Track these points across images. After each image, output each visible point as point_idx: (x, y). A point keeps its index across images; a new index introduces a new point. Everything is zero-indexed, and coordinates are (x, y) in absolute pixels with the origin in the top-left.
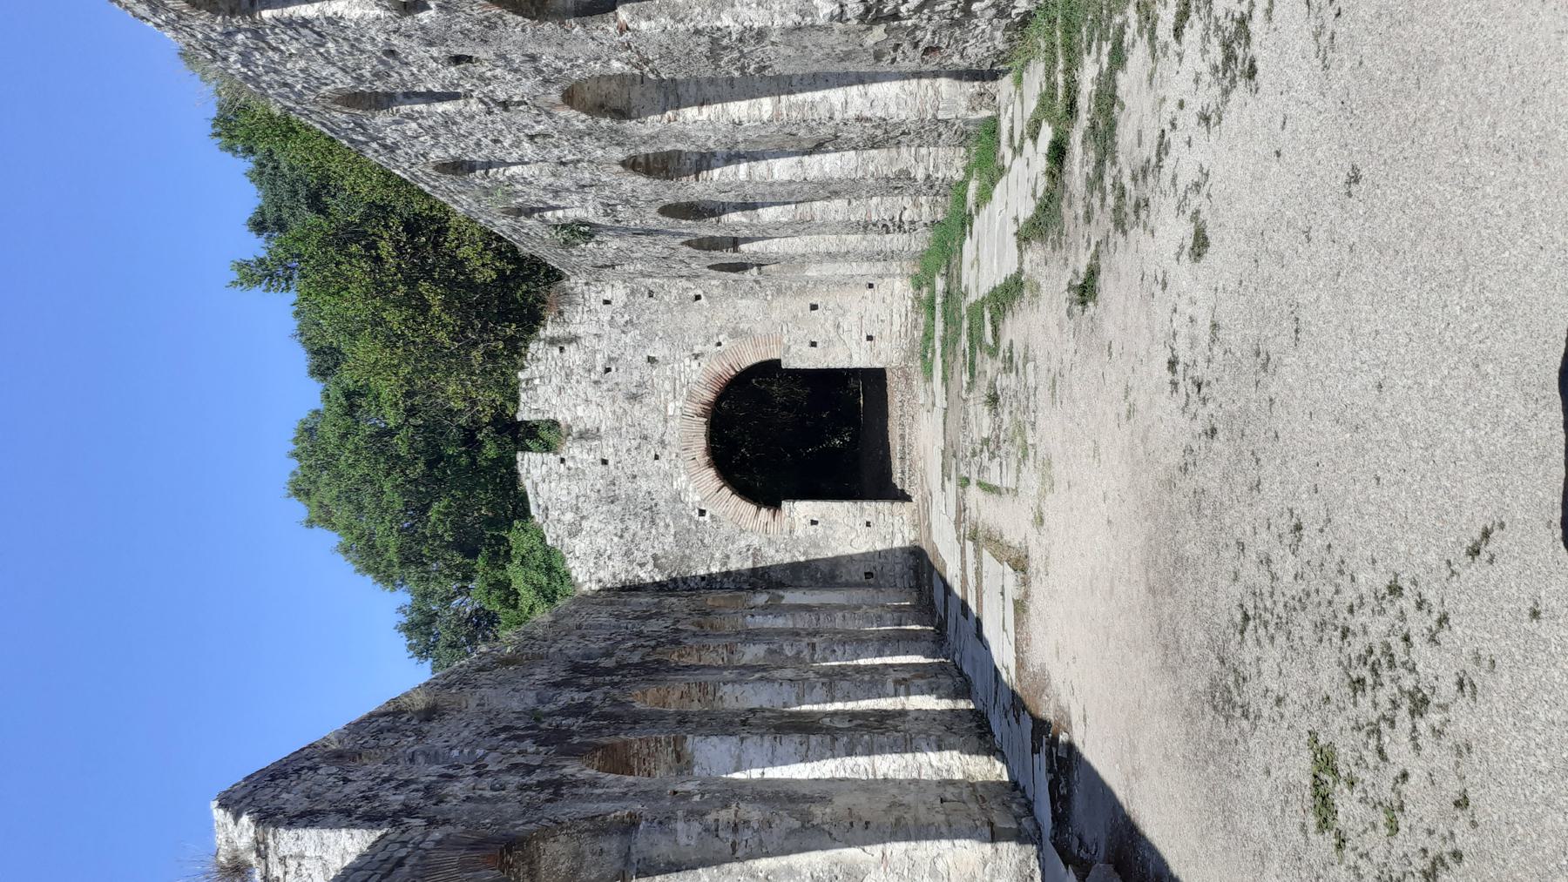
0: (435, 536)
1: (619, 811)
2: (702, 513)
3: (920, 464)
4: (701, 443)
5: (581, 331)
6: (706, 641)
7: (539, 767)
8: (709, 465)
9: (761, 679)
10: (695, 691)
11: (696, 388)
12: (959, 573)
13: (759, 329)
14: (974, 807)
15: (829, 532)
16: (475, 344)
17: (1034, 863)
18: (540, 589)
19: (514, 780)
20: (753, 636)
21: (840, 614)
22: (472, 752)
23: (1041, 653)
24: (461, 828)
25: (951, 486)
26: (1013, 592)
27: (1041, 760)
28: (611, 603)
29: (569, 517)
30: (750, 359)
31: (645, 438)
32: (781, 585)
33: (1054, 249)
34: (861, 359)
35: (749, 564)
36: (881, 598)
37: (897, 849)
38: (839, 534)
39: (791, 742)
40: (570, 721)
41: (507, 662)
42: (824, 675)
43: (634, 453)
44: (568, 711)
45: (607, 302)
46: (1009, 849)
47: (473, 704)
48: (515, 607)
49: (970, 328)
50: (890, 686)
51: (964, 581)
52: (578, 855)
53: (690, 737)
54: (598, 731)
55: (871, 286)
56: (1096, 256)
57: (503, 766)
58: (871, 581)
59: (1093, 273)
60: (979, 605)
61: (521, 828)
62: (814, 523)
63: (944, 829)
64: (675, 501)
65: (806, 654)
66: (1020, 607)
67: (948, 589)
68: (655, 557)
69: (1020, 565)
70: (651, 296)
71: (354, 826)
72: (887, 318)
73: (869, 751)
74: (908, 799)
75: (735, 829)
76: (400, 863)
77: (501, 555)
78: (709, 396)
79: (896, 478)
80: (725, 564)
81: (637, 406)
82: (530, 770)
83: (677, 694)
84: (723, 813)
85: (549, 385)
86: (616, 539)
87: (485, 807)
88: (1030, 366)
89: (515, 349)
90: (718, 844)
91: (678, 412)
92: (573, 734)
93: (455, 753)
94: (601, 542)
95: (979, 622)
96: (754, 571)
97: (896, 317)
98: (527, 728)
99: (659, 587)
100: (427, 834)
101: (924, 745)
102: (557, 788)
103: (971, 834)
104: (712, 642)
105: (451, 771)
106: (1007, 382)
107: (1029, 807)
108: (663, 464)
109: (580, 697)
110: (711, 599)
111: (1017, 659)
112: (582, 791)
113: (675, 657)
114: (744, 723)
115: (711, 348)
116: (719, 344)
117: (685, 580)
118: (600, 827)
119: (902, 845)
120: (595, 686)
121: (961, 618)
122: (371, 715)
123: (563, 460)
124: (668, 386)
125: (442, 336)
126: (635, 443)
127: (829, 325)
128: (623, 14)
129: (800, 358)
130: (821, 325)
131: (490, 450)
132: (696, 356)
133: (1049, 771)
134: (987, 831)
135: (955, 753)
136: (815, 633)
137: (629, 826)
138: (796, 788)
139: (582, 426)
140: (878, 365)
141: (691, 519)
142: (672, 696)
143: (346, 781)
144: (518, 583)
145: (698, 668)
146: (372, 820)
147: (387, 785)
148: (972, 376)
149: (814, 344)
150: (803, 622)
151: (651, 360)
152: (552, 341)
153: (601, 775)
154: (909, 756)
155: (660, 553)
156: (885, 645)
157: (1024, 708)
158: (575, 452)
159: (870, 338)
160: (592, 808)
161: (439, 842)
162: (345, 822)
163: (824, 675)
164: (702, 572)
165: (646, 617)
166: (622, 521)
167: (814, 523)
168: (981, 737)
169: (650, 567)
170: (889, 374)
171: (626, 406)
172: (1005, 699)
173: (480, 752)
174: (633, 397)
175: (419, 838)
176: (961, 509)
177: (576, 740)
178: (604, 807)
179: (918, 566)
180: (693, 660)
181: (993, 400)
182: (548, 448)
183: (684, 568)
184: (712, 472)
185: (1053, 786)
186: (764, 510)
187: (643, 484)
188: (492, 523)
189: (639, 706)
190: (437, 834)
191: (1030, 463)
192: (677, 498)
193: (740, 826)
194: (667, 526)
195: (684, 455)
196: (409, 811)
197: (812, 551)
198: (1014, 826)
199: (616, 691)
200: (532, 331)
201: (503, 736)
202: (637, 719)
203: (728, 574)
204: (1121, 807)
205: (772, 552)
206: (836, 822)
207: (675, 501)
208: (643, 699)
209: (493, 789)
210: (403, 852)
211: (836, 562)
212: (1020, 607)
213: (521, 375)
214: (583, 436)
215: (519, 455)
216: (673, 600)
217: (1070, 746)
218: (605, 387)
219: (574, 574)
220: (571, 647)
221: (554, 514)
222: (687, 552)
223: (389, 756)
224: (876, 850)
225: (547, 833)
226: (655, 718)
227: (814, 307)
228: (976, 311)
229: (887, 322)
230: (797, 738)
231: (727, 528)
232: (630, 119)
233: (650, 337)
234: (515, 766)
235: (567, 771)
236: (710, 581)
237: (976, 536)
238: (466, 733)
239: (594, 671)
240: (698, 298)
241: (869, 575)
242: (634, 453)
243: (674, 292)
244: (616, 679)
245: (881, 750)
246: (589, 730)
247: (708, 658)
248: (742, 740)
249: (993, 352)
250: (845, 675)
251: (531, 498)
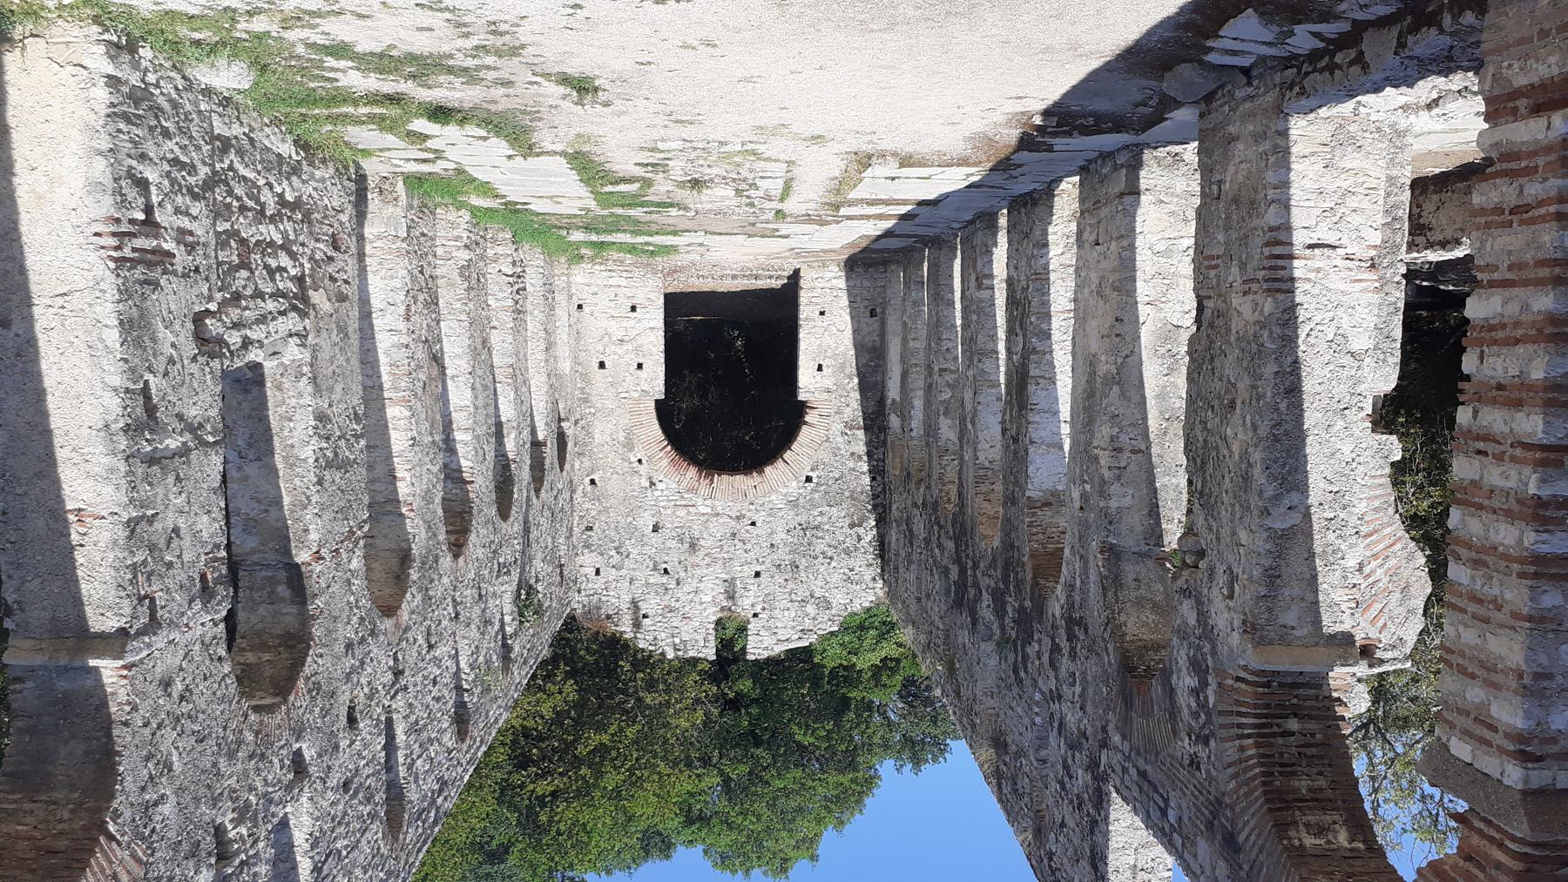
0: (828, 738)
1: (1097, 562)
3: (762, 259)
4: (739, 480)
5: (627, 598)
6: (935, 477)
7: (1053, 640)
8: (761, 472)
9: (973, 423)
10: (983, 488)
11: (684, 484)
12: (872, 222)
13: (624, 421)
14: (1104, 212)
16: (640, 700)
17: (1161, 152)
18: (881, 637)
19: (1065, 664)
20: (931, 430)
21: (911, 343)
22: (1037, 703)
23: (953, 141)
24: (1111, 716)
25: (785, 228)
26: (891, 168)
27: (1059, 143)
28: (896, 568)
29: (811, 609)
30: (655, 431)
31: (734, 535)
32: (881, 401)
33: (540, 119)
34: (655, 318)
35: (861, 434)
36: (896, 302)
37: (1143, 290)
39: (1035, 394)
40: (1009, 609)
41: (951, 670)
42: (971, 360)
43: (748, 546)
44: (1000, 611)
45: (598, 572)
46: (1146, 178)
47: (991, 703)
48: (898, 661)
49: (623, 206)
50: (985, 294)
51: (880, 217)
52: (1140, 603)
53: (1028, 494)
54: (1019, 583)
55: (580, 307)
56: (547, 76)
57: (1052, 674)
58: (878, 310)
59: (565, 80)
60: (904, 202)
61: (1111, 658)
62: (820, 368)
63: (1125, 243)
64: (796, 506)
65: (949, 378)
66: (906, 161)
67: (888, 234)
68: (852, 526)
69: (864, 161)
70: (591, 529)
71: (1107, 817)
72: (611, 293)
73: (1047, 316)
74: (1094, 277)
75: (1118, 450)
76: (1143, 774)
77: (846, 675)
78: (692, 472)
79: (776, 284)
81: (702, 542)
82: (1056, 649)
83: (986, 504)
84: (1102, 462)
85: (680, 629)
87: (1090, 691)
88: (660, 145)
89: (645, 661)
90: (1133, 468)
91: (708, 502)
92: (1022, 607)
93: (1038, 720)
94: (835, 578)
95: (921, 203)
96: (866, 428)
97: (611, 282)
98: (1016, 651)
99: (881, 522)
100: (1116, 748)
101: (1043, 261)
102: (1074, 623)
103: (1130, 215)
105: (1056, 725)
106: (678, 169)
107: (1106, 156)
108: (759, 518)
109: (986, 599)
110: (894, 470)
111: (959, 165)
112: (1077, 598)
113: (950, 507)
114: (1016, 440)
115: (643, 469)
117: (875, 497)
118: (1113, 581)
119: (1139, 284)
120: (976, 585)
121: (917, 221)
122: (1000, 800)
123: (755, 615)
124: (682, 512)
125: (631, 732)
126: (739, 545)
127: (620, 350)
128: (302, 557)
129: (654, 381)
130: (620, 359)
131: (745, 685)
132: (652, 484)
133: (1070, 135)
134: (1128, 199)
135: (1050, 229)
136: (929, 368)
137: (1112, 553)
138: (1080, 390)
139: (722, 597)
140: (662, 301)
142: (987, 510)
143: (1063, 825)
144: (875, 658)
145: (961, 485)
146: (1101, 801)
147: (1068, 786)
148: (671, 205)
149: (640, 366)
150: (918, 381)
151: (656, 529)
152: (637, 625)
153: (1062, 580)
154: (1052, 276)
155: (848, 521)
156: (942, 299)
157: (1008, 159)
158: (746, 604)
159: (633, 309)
160: (1094, 589)
161: (1124, 737)
162: (1102, 826)
163: (971, 360)
164: (867, 480)
165: (910, 535)
166: (815, 558)
167: (820, 368)
168: (1035, 203)
169: (861, 531)
170: (670, 290)
171: (701, 553)
172: (998, 179)
173: (1038, 696)
174: (693, 546)
175: (1119, 755)
176: (808, 219)
177: (1028, 603)
178: (1093, 578)
179: (865, 264)
180: (953, 489)
181: (696, 184)
182: (742, 629)
183: (863, 497)
184: (768, 470)
185: (1086, 131)
186: (807, 418)
187: (777, 539)
188: (816, 683)
189: (996, 543)
190: (1117, 739)
191: (761, 148)
192: (794, 504)
193: (1116, 445)
195: (751, 496)
196: (1093, 765)
197: (847, 371)
198: (1124, 171)
199: (982, 565)
200: (626, 645)
201: (1022, 674)
202: (1009, 545)
203: (869, 454)
204: (1108, 63)
205: (849, 410)
206: (1114, 351)
207: (796, 506)
208: (990, 538)
209: (1073, 684)
210: (1133, 771)
211: (858, 346)
212: (906, 161)
213: (670, 655)
214: (731, 596)
215: (750, 657)
216: (894, 507)
217: (1046, 113)
218: (683, 574)
219: (867, 604)
220: (937, 608)
221: (808, 624)
222: (847, 494)
223: (1040, 784)
224: (1143, 311)
225: (1117, 632)
226: (1009, 527)
227: (602, 365)
228: (604, 200)
229: (620, 291)
230: (1031, 388)
231: (824, 455)
232: (410, 549)
233: (632, 530)
234: (1052, 663)
235: (1058, 613)
236: (877, 472)
237: (835, 206)
238: (1019, 710)
239: (961, 585)
240: (593, 482)
241: (873, 314)
242: (748, 546)
243: (587, 506)
244: (970, 564)
245: (1046, 304)
246: (1019, 591)
247: (952, 475)
248: (1032, 442)
249: (648, 183)
251: (791, 646)
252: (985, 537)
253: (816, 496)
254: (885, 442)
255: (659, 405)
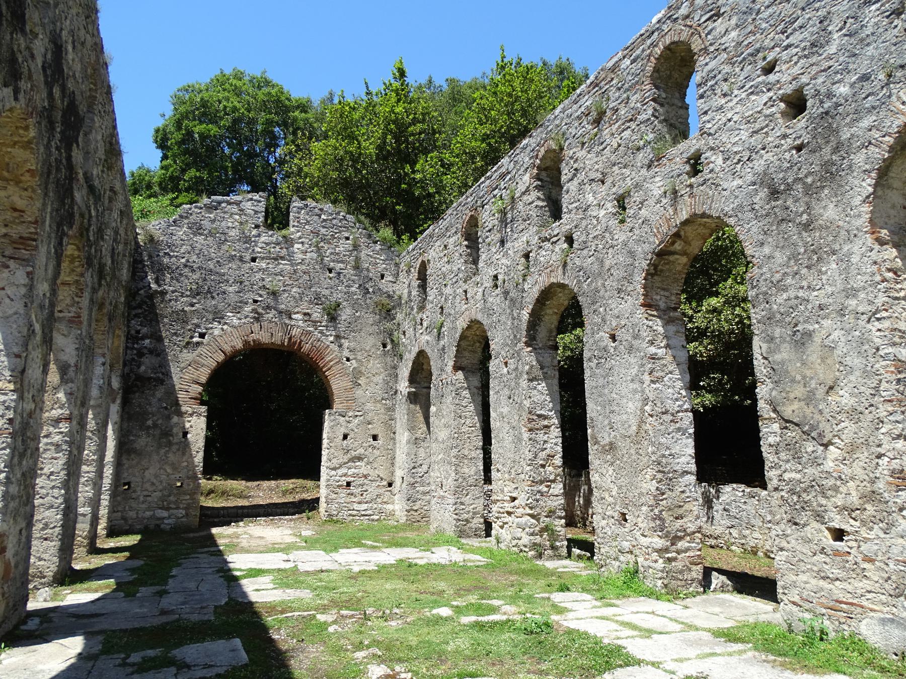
2: (202, 336)
13: (359, 392)
15: (174, 448)
30: (338, 384)
32: (125, 403)
38: (171, 457)
55: (390, 485)
68: (163, 293)
80: (151, 352)
83: (20, 203)
86: (183, 260)
97: (365, 506)
104: (85, 302)
115: (346, 353)
116: (348, 360)
123: (257, 227)
141: (198, 326)
149: (345, 437)
155: (168, 297)
159: (348, 484)
180: (64, 277)
184: (239, 345)
192: (218, 317)
194: (192, 305)
227: (375, 438)
233: (355, 306)
240: (384, 346)
250: (22, 455)
252: (27, 145)
253: (195, 321)
254: (125, 365)
255: (330, 407)
